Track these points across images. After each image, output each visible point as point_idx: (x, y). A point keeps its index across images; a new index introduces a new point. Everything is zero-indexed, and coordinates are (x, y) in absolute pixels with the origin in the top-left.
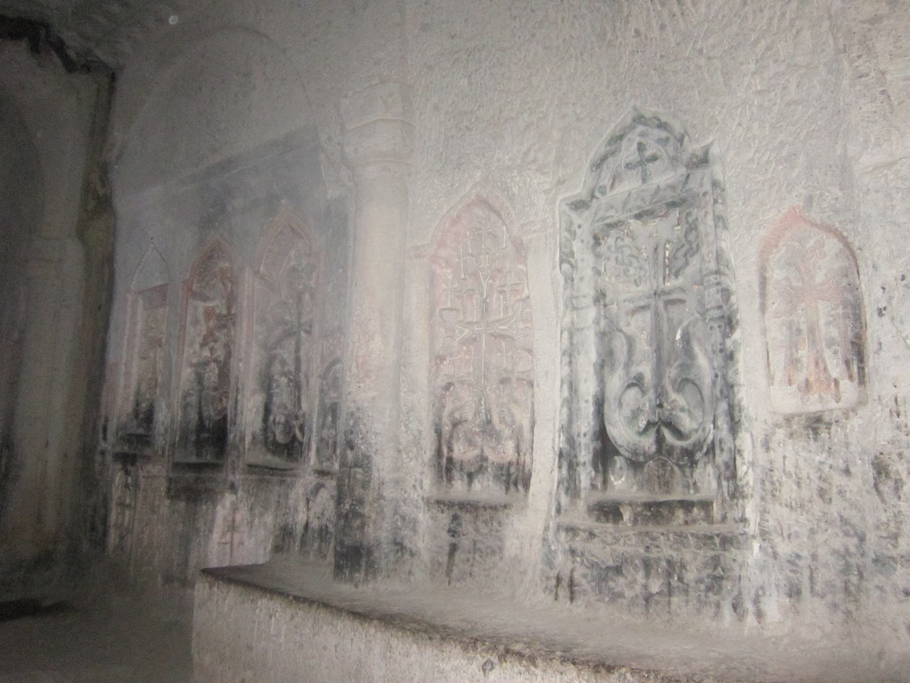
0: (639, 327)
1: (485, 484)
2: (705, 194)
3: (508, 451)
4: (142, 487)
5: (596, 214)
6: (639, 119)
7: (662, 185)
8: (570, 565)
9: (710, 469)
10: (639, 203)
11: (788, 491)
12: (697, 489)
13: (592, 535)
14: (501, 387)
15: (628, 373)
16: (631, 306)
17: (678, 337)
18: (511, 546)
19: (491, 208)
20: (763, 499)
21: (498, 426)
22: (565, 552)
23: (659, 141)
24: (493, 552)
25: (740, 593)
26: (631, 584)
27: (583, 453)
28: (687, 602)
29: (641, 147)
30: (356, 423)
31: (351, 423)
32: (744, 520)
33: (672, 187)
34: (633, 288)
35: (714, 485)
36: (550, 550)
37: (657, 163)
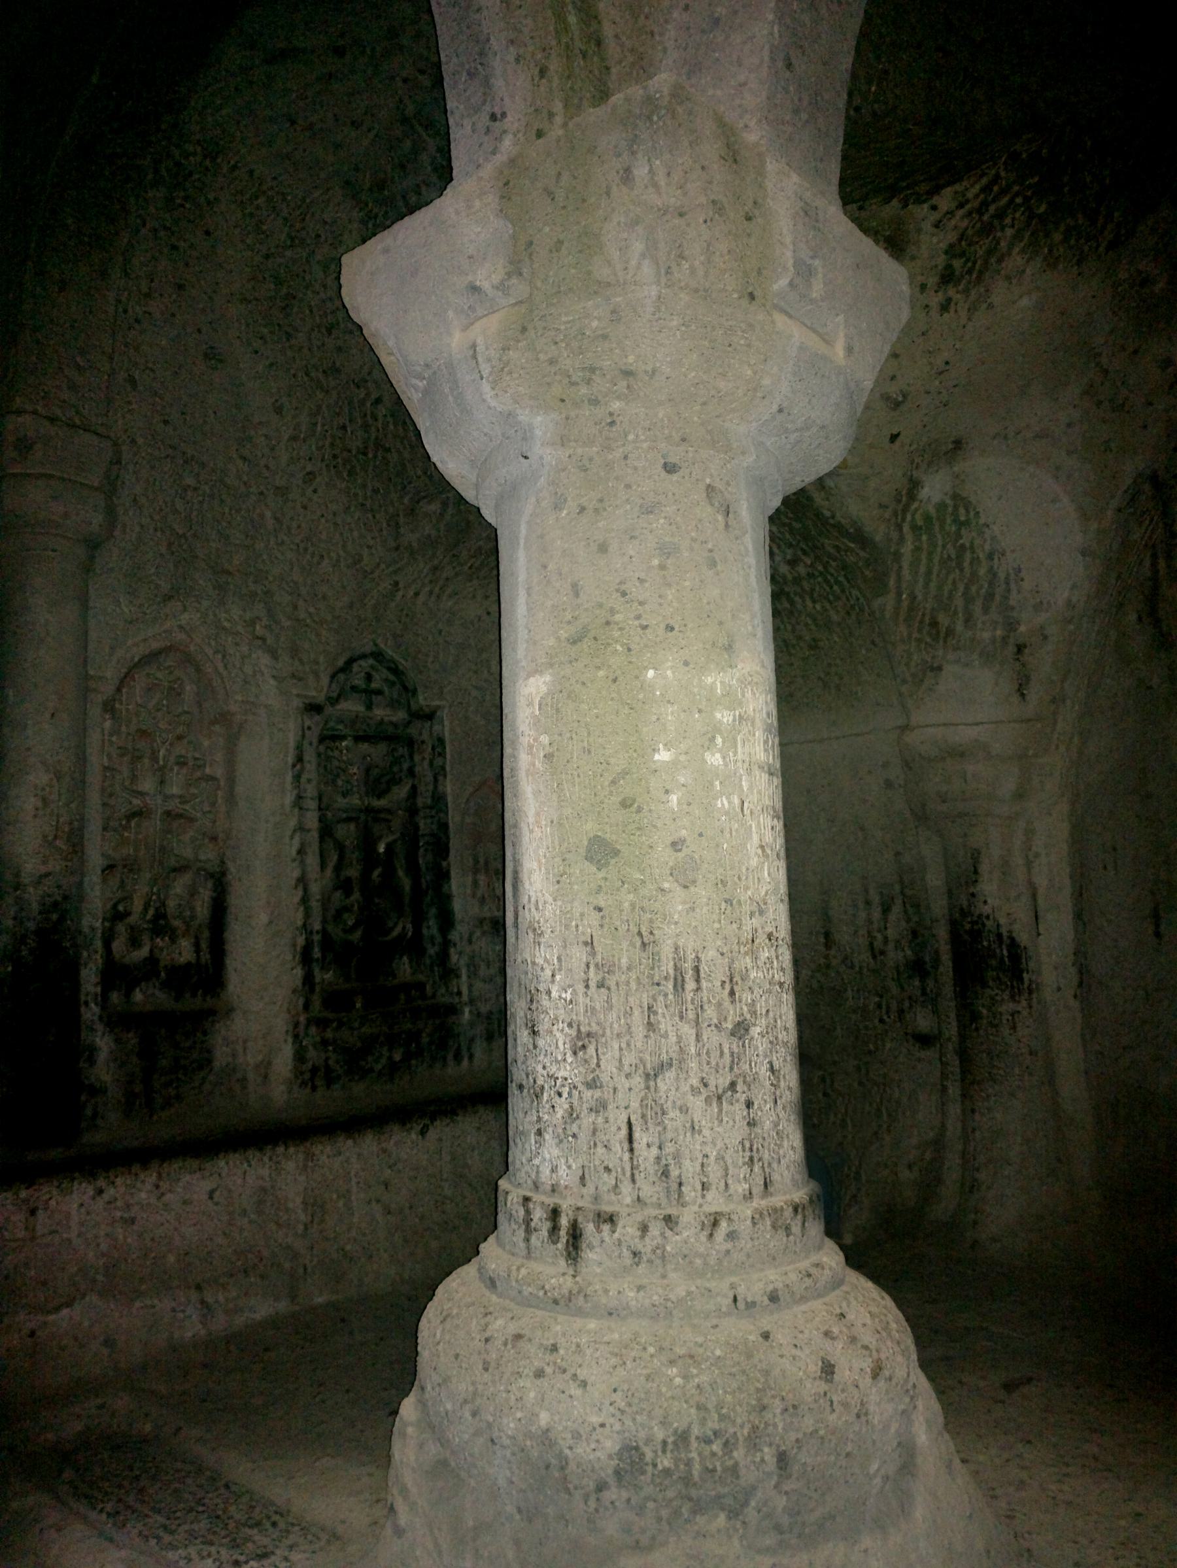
0: (347, 833)
1: (150, 992)
2: (423, 742)
3: (184, 952)
5: (326, 722)
6: (378, 655)
7: (386, 719)
8: (323, 1056)
9: (405, 958)
10: (364, 727)
11: (483, 971)
12: (395, 976)
13: (341, 1024)
14: (172, 875)
15: (338, 876)
16: (344, 815)
17: (382, 850)
18: (221, 1058)
19: (188, 659)
20: (469, 977)
21: (176, 923)
22: (314, 1046)
23: (386, 680)
24: (201, 1068)
25: (459, 1045)
26: (377, 1061)
27: (316, 950)
28: (422, 1062)
29: (369, 677)
30: (62, 919)
31: (55, 917)
32: (459, 993)
33: (395, 725)
34: (340, 799)
35: (409, 970)
36: (301, 1046)
37: (380, 698)
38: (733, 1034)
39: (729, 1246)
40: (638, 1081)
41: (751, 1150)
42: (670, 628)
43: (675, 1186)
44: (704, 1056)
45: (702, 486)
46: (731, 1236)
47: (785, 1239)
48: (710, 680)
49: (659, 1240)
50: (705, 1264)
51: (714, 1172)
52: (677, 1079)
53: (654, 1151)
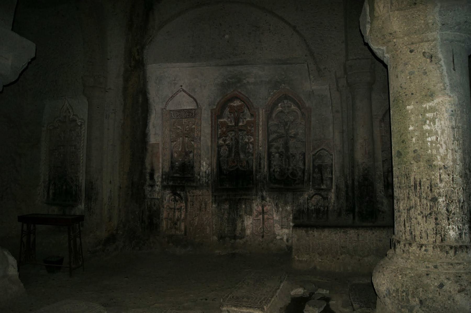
4: (189, 200)
38: (431, 200)
39: (425, 253)
40: (406, 211)
41: (436, 230)
42: (412, 94)
43: (413, 237)
44: (422, 206)
45: (422, 53)
46: (426, 250)
47: (446, 255)
48: (424, 106)
49: (408, 248)
50: (419, 256)
51: (424, 235)
52: (415, 211)
53: (409, 228)
